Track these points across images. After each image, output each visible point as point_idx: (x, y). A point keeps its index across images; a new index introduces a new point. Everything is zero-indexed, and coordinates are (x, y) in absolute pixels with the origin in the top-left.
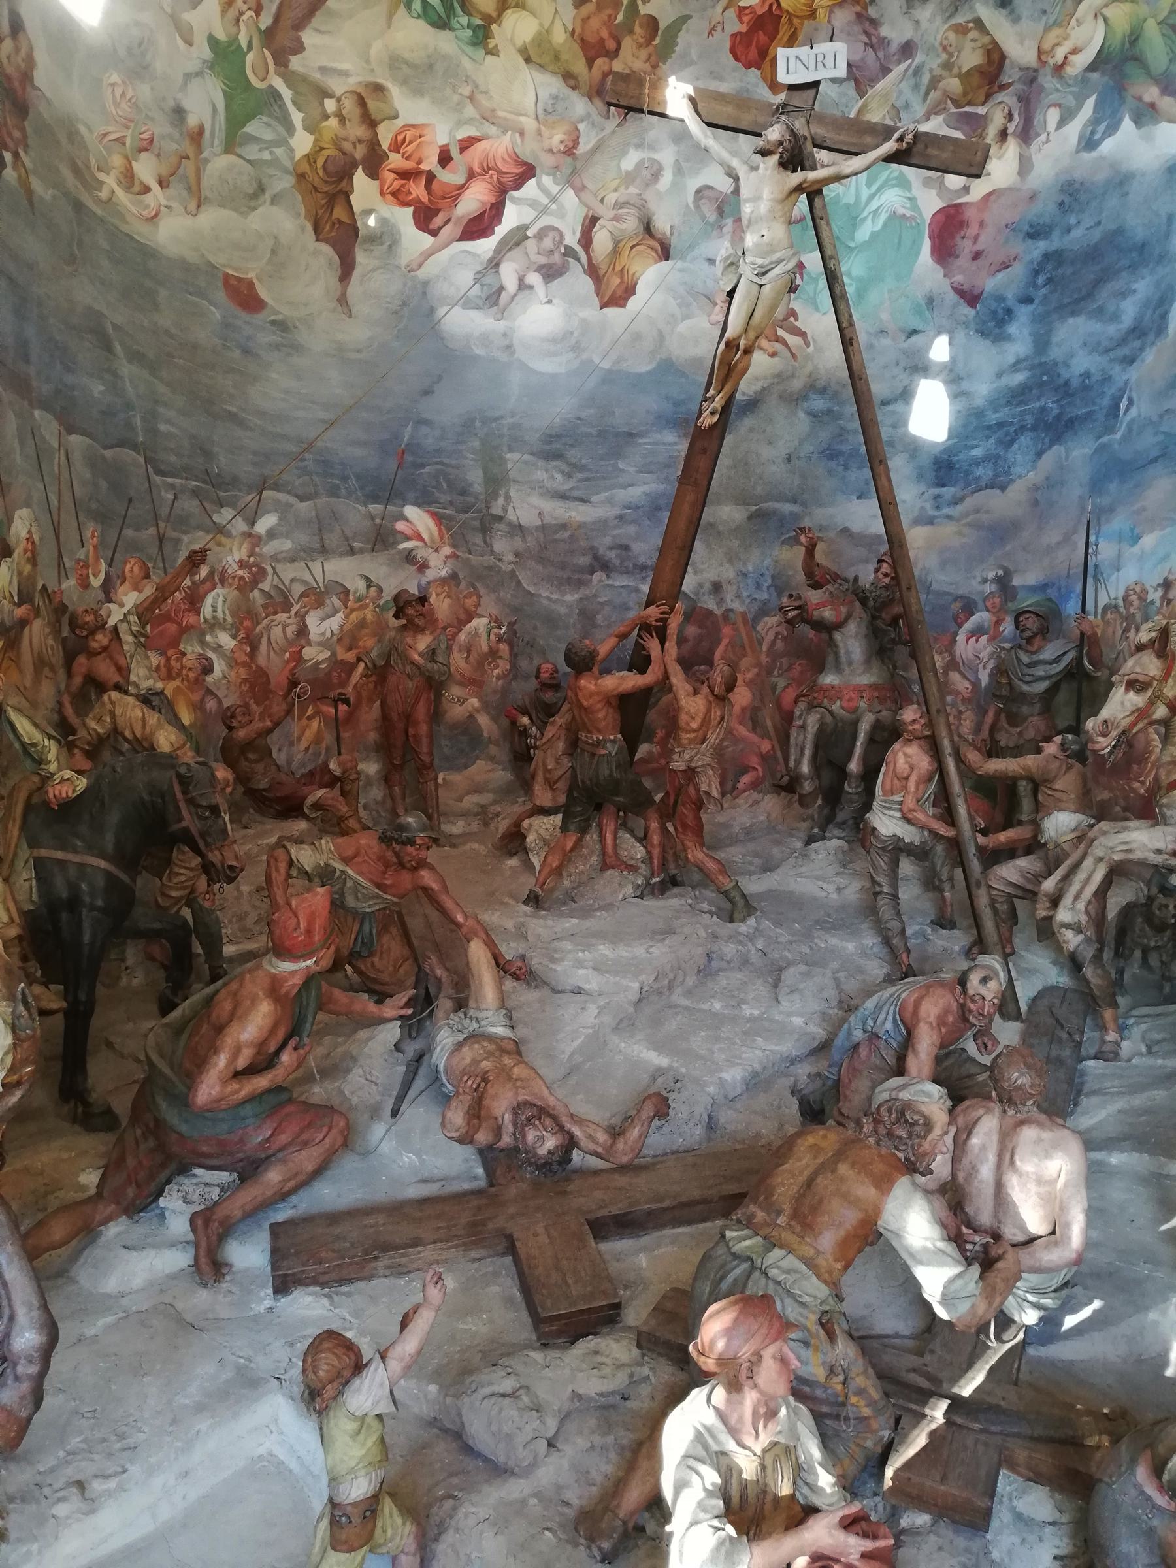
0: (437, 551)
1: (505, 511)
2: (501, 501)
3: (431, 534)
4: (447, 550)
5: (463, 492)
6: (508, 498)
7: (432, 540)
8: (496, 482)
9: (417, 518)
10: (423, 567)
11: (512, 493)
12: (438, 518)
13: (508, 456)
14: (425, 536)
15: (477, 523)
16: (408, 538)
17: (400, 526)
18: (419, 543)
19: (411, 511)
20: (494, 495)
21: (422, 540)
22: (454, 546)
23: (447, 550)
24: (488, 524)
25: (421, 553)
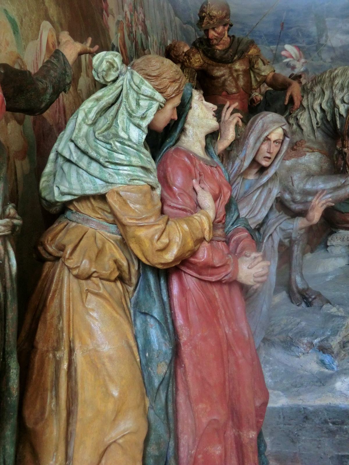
0: (298, 61)
1: (326, 41)
2: (324, 38)
3: (296, 55)
4: (303, 60)
5: (309, 36)
6: (327, 36)
7: (296, 57)
8: (322, 31)
9: (290, 49)
10: (293, 68)
11: (329, 34)
12: (299, 48)
13: (326, 19)
14: (294, 56)
15: (315, 48)
16: (287, 57)
17: (283, 53)
18: (291, 59)
19: (288, 47)
20: (320, 36)
21: (292, 57)
22: (306, 58)
23: (303, 60)
24: (319, 47)
25: (292, 63)
